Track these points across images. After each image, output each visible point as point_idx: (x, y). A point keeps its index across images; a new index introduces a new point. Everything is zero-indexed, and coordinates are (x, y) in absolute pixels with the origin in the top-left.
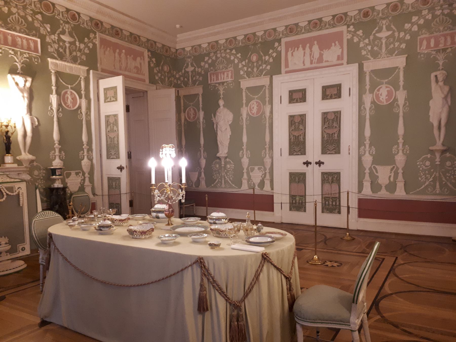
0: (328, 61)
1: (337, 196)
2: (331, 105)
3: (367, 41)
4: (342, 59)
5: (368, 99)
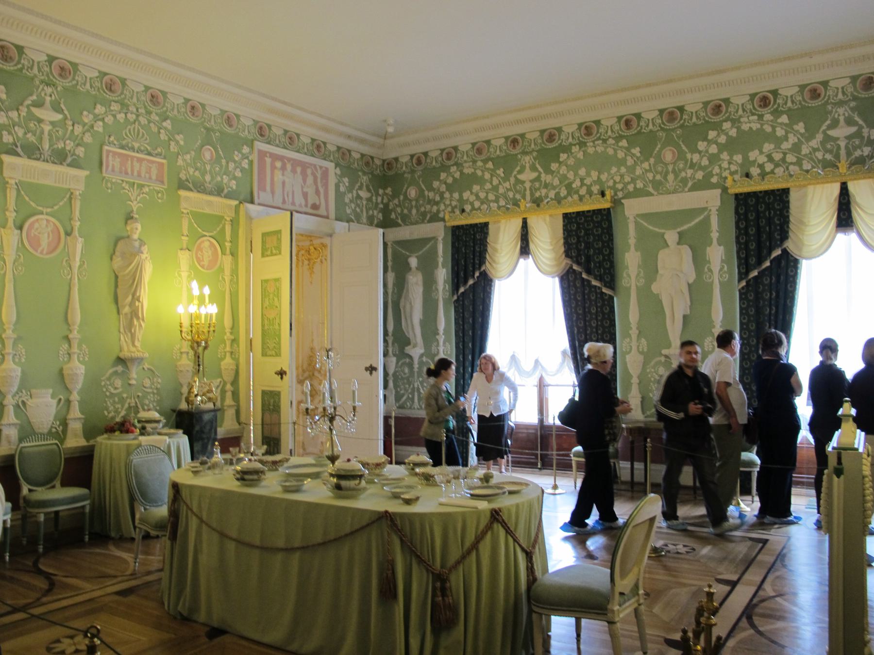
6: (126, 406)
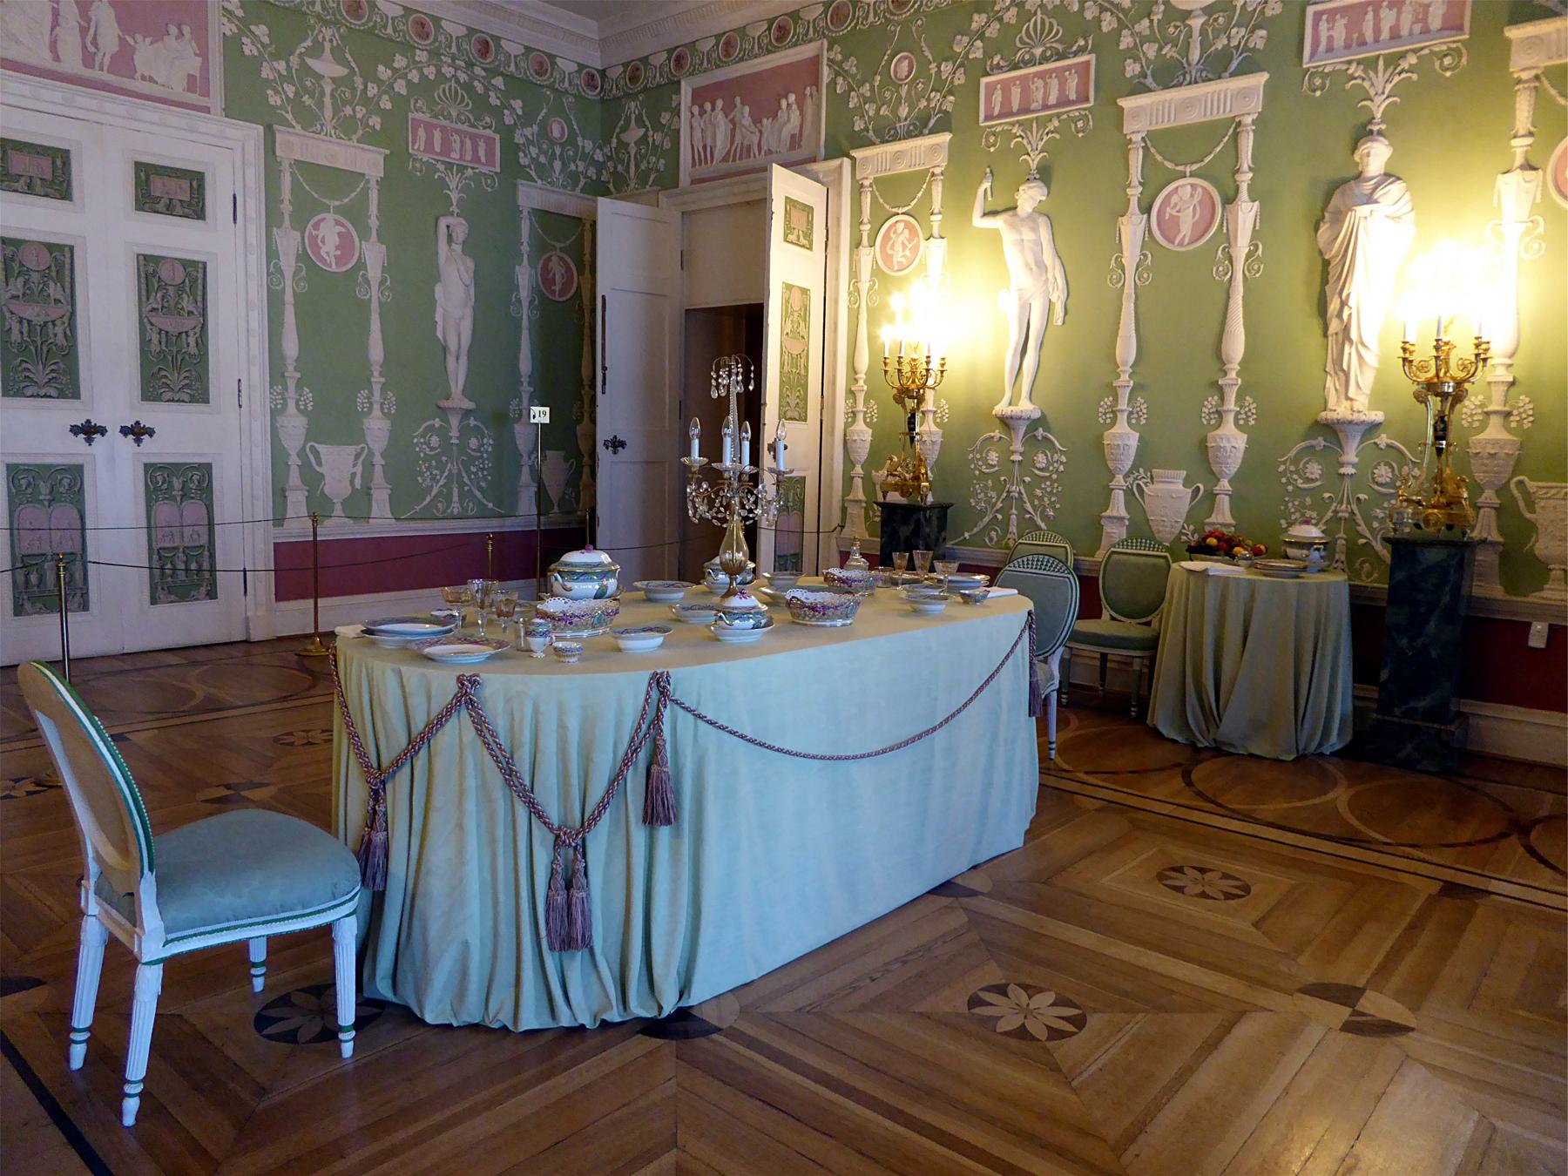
0: (151, 80)
1: (204, 540)
2: (172, 237)
3: (281, 66)
4: (206, 93)
5: (288, 242)
6: (1330, 514)
